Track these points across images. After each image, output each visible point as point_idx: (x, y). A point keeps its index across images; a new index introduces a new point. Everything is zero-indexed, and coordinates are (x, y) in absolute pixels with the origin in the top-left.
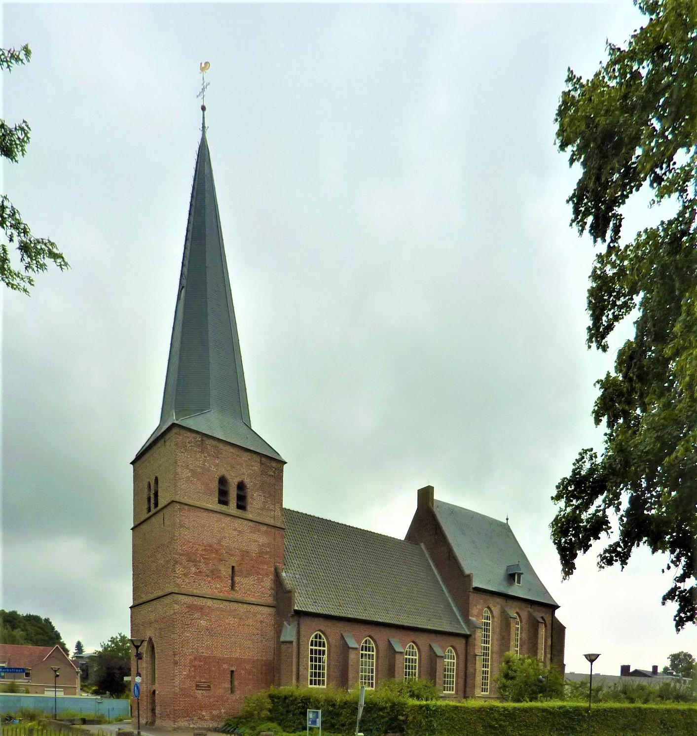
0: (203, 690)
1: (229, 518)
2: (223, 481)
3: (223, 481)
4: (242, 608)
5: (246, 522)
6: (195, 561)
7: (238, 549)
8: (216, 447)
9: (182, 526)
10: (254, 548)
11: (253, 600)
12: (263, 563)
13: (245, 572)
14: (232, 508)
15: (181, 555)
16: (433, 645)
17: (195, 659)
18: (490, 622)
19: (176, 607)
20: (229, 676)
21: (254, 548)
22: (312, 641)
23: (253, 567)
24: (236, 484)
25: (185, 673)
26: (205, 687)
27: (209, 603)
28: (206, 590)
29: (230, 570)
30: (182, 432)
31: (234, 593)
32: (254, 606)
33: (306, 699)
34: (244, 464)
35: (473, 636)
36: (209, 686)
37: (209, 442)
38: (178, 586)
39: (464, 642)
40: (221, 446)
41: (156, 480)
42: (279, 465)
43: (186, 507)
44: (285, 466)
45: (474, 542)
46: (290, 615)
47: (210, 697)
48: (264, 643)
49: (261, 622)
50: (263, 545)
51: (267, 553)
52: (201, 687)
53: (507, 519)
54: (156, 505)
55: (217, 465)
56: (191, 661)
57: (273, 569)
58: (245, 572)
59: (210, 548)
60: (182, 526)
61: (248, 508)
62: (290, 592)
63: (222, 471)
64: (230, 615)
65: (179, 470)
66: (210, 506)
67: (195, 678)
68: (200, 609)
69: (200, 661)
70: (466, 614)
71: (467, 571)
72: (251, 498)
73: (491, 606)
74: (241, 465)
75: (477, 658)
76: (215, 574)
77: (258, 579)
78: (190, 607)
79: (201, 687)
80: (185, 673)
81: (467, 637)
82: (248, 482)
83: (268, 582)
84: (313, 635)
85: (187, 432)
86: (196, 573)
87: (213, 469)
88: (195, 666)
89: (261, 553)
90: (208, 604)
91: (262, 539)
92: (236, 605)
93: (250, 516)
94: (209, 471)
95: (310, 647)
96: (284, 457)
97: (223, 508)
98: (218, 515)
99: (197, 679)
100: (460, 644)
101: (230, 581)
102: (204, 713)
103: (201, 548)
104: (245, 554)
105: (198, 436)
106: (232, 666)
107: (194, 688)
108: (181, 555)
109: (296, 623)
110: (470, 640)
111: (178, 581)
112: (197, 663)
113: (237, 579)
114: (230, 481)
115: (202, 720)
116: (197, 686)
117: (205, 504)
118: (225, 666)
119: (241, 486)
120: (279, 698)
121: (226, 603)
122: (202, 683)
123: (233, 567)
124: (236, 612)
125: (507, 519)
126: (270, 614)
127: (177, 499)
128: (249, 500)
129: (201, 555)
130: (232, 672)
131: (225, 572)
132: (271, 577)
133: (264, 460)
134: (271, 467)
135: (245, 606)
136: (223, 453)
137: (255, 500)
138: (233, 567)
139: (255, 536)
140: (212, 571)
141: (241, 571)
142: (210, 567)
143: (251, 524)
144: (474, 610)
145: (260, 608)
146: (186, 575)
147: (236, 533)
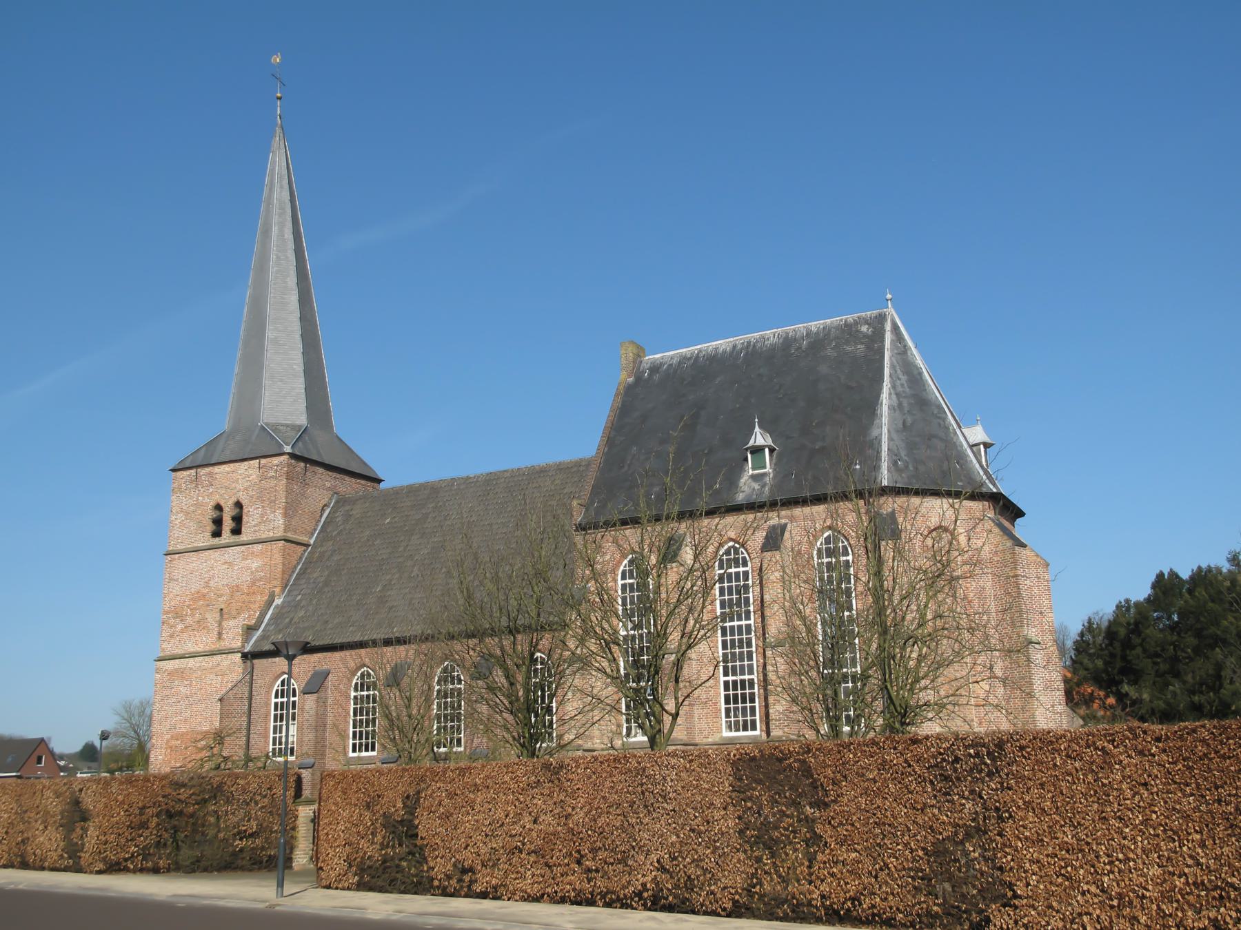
1: (218, 551)
3: (219, 508)
13: (234, 613)
17: (172, 736)
22: (277, 691)
23: (244, 602)
25: (160, 757)
28: (192, 648)
43: (177, 556)
56: (168, 741)
58: (234, 613)
59: (200, 596)
63: (216, 499)
68: (180, 673)
69: (177, 740)
77: (250, 616)
80: (160, 757)
84: (279, 682)
87: (207, 500)
88: (171, 747)
89: (253, 582)
92: (218, 658)
95: (296, 699)
97: (217, 541)
103: (188, 598)
104: (235, 589)
112: (173, 742)
119: (239, 505)
131: (212, 618)
133: (263, 461)
135: (230, 656)
141: (229, 613)
142: (198, 617)
146: (171, 636)
147: (225, 567)
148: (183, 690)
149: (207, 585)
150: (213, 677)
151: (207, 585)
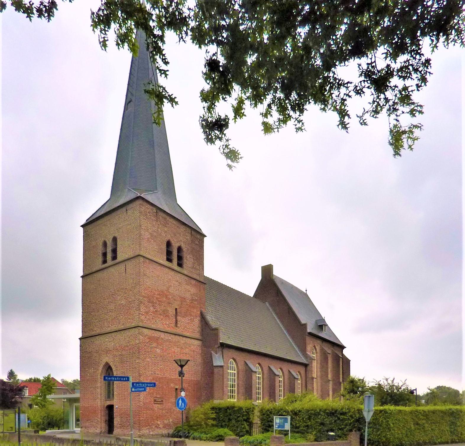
0: (158, 404)
2: (169, 244)
3: (169, 244)
4: (183, 340)
5: (183, 277)
6: (152, 302)
7: (179, 296)
8: (165, 219)
9: (145, 275)
10: (188, 296)
11: (188, 334)
12: (194, 307)
14: (174, 265)
15: (144, 297)
16: (291, 371)
18: (315, 356)
19: (141, 337)
20: (174, 392)
21: (188, 296)
24: (177, 247)
26: (160, 402)
27: (162, 335)
28: (160, 326)
29: (174, 311)
30: (145, 204)
31: (177, 328)
32: (189, 339)
33: (248, 409)
34: (182, 233)
35: (310, 365)
36: (162, 401)
37: (161, 214)
38: (142, 321)
39: (304, 369)
40: (168, 218)
41: (115, 240)
42: (201, 238)
43: (147, 261)
44: (205, 238)
45: (297, 303)
46: (216, 346)
47: (162, 409)
48: (195, 367)
49: (194, 351)
50: (194, 294)
51: (196, 300)
52: (157, 401)
53: (306, 291)
54: (114, 258)
55: (165, 232)
57: (199, 312)
59: (162, 294)
60: (145, 275)
61: (184, 266)
62: (216, 329)
63: (168, 237)
64: (175, 345)
65: (143, 232)
66: (162, 262)
67: (153, 394)
68: (157, 339)
70: (303, 350)
71: (303, 322)
72: (186, 259)
73: (316, 345)
74: (180, 234)
75: (314, 380)
76: (165, 314)
78: (151, 339)
79: (157, 401)
81: (306, 365)
82: (183, 246)
83: (197, 321)
85: (147, 204)
86: (153, 312)
90: (162, 337)
91: (193, 290)
93: (185, 272)
94: (161, 235)
96: (204, 232)
98: (167, 270)
99: (155, 395)
100: (302, 369)
101: (174, 319)
102: (159, 423)
104: (183, 299)
105: (154, 208)
106: (176, 385)
107: (153, 403)
108: (144, 297)
109: (221, 352)
110: (308, 368)
111: (143, 317)
113: (179, 318)
114: (173, 244)
115: (158, 428)
116: (155, 401)
117: (158, 260)
118: (172, 385)
119: (180, 249)
120: (220, 409)
121: (173, 336)
122: (157, 398)
123: (176, 309)
124: (179, 344)
125: (306, 291)
126: (199, 346)
127: (142, 253)
128: (185, 260)
129: (157, 298)
130: (176, 389)
131: (172, 312)
132: (199, 318)
134: (197, 239)
135: (184, 339)
136: (170, 224)
137: (188, 260)
138: (176, 309)
139: (188, 287)
140: (164, 311)
142: (163, 308)
143: (186, 278)
144: (309, 347)
145: (193, 341)
146: (147, 313)
147: (177, 283)
148: (158, 351)
149: (168, 290)
150: (176, 348)
151: (168, 290)
